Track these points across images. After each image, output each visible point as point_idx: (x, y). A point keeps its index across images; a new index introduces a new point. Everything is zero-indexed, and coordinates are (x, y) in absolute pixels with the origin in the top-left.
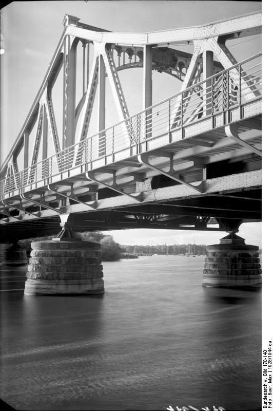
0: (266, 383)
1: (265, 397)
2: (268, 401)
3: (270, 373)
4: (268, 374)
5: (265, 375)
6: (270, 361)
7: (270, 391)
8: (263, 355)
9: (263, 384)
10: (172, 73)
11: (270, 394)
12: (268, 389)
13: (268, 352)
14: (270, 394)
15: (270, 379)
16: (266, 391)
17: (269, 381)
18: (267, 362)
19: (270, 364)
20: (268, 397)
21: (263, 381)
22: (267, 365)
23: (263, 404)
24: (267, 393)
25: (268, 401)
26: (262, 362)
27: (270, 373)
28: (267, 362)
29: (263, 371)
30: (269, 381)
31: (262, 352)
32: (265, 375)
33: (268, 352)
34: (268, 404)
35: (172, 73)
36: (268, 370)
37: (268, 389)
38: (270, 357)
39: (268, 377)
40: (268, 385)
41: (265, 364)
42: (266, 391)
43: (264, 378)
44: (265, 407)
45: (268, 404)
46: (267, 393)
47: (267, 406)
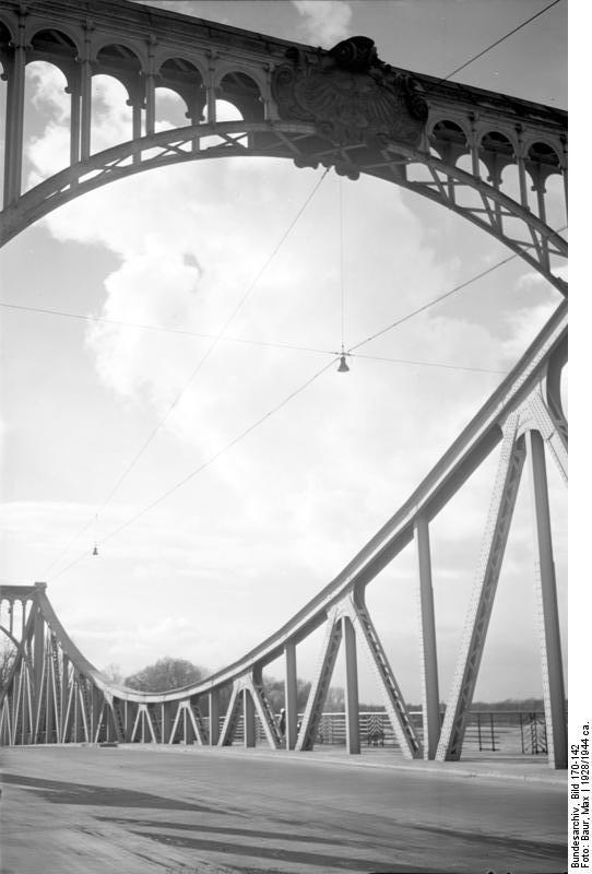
0: (577, 815)
1: (576, 844)
2: (581, 853)
3: (586, 794)
4: (581, 794)
5: (576, 797)
6: (585, 767)
7: (586, 831)
8: (570, 754)
9: (570, 817)
10: (410, 178)
11: (586, 839)
12: (581, 828)
13: (581, 749)
14: (586, 839)
15: (586, 805)
16: (577, 831)
17: (583, 810)
18: (580, 770)
19: (585, 774)
20: (582, 844)
21: (571, 811)
22: (580, 775)
23: (571, 860)
24: (580, 836)
25: (581, 853)
26: (570, 769)
27: (586, 794)
28: (580, 770)
29: (570, 788)
30: (583, 810)
31: (570, 749)
32: (576, 797)
33: (581, 749)
34: (581, 859)
35: (410, 178)
36: (582, 787)
37: (581, 828)
38: (585, 760)
39: (581, 801)
40: (582, 818)
41: (575, 774)
42: (577, 831)
43: (572, 804)
44: (575, 866)
45: (581, 859)
46: (580, 836)
47: (580, 863)
